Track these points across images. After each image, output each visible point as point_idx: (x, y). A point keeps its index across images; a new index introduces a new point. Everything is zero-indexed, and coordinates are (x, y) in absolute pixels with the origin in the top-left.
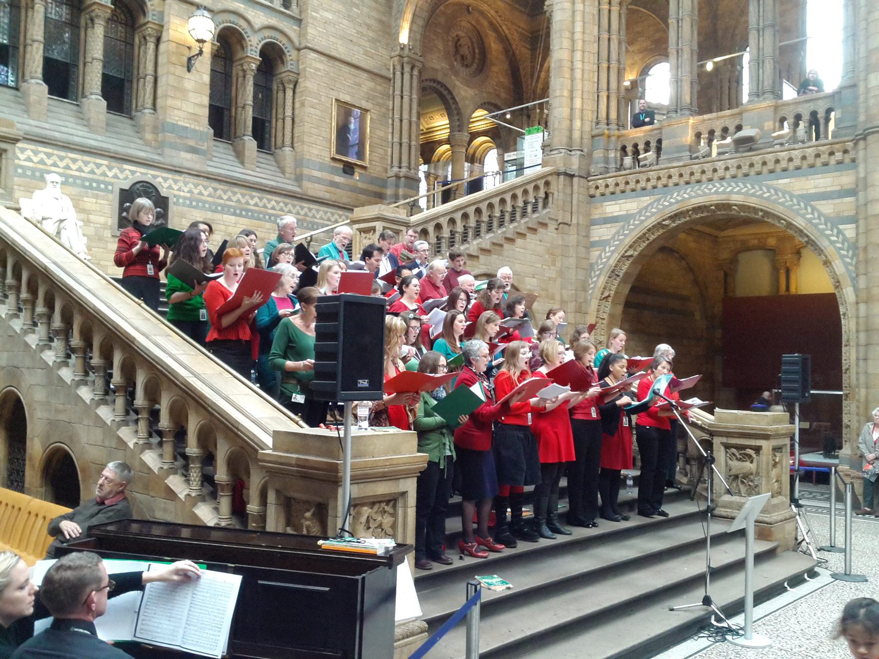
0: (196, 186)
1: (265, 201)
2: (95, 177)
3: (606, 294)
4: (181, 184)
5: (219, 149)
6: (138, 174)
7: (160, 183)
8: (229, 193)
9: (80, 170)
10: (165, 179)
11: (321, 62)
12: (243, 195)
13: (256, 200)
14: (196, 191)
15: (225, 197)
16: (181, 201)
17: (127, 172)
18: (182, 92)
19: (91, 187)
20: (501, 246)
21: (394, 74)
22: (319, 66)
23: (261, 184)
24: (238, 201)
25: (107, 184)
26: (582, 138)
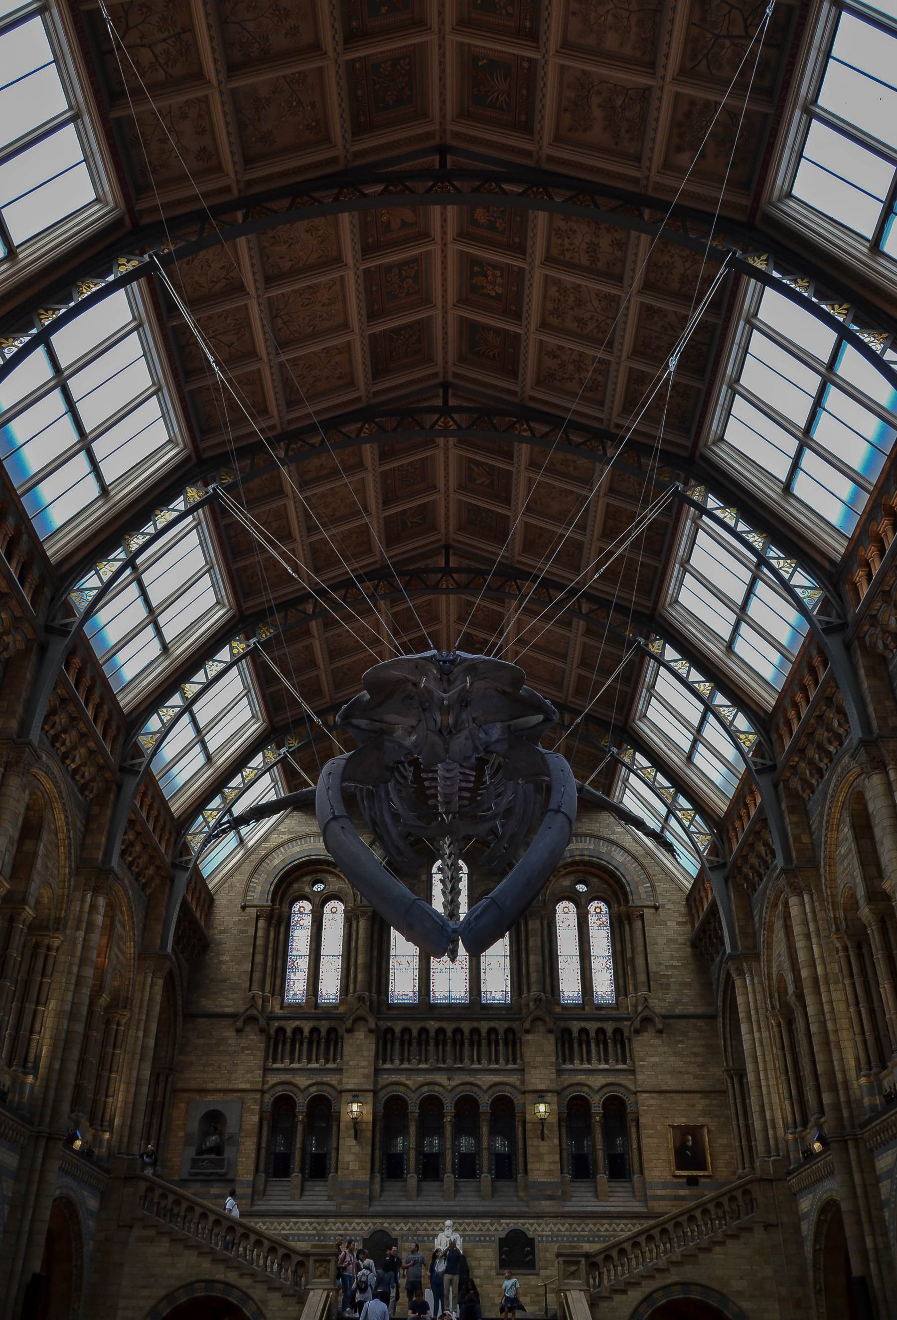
0: (555, 1225)
1: (614, 1225)
4: (543, 1226)
7: (528, 1228)
8: (583, 1225)
10: (532, 1224)
11: (653, 1098)
12: (595, 1225)
13: (606, 1226)
14: (555, 1229)
15: (579, 1229)
16: (544, 1239)
17: (504, 1225)
18: (539, 1157)
19: (480, 1241)
22: (651, 1102)
23: (609, 1212)
24: (591, 1230)
25: (490, 1236)
26: (777, 1144)
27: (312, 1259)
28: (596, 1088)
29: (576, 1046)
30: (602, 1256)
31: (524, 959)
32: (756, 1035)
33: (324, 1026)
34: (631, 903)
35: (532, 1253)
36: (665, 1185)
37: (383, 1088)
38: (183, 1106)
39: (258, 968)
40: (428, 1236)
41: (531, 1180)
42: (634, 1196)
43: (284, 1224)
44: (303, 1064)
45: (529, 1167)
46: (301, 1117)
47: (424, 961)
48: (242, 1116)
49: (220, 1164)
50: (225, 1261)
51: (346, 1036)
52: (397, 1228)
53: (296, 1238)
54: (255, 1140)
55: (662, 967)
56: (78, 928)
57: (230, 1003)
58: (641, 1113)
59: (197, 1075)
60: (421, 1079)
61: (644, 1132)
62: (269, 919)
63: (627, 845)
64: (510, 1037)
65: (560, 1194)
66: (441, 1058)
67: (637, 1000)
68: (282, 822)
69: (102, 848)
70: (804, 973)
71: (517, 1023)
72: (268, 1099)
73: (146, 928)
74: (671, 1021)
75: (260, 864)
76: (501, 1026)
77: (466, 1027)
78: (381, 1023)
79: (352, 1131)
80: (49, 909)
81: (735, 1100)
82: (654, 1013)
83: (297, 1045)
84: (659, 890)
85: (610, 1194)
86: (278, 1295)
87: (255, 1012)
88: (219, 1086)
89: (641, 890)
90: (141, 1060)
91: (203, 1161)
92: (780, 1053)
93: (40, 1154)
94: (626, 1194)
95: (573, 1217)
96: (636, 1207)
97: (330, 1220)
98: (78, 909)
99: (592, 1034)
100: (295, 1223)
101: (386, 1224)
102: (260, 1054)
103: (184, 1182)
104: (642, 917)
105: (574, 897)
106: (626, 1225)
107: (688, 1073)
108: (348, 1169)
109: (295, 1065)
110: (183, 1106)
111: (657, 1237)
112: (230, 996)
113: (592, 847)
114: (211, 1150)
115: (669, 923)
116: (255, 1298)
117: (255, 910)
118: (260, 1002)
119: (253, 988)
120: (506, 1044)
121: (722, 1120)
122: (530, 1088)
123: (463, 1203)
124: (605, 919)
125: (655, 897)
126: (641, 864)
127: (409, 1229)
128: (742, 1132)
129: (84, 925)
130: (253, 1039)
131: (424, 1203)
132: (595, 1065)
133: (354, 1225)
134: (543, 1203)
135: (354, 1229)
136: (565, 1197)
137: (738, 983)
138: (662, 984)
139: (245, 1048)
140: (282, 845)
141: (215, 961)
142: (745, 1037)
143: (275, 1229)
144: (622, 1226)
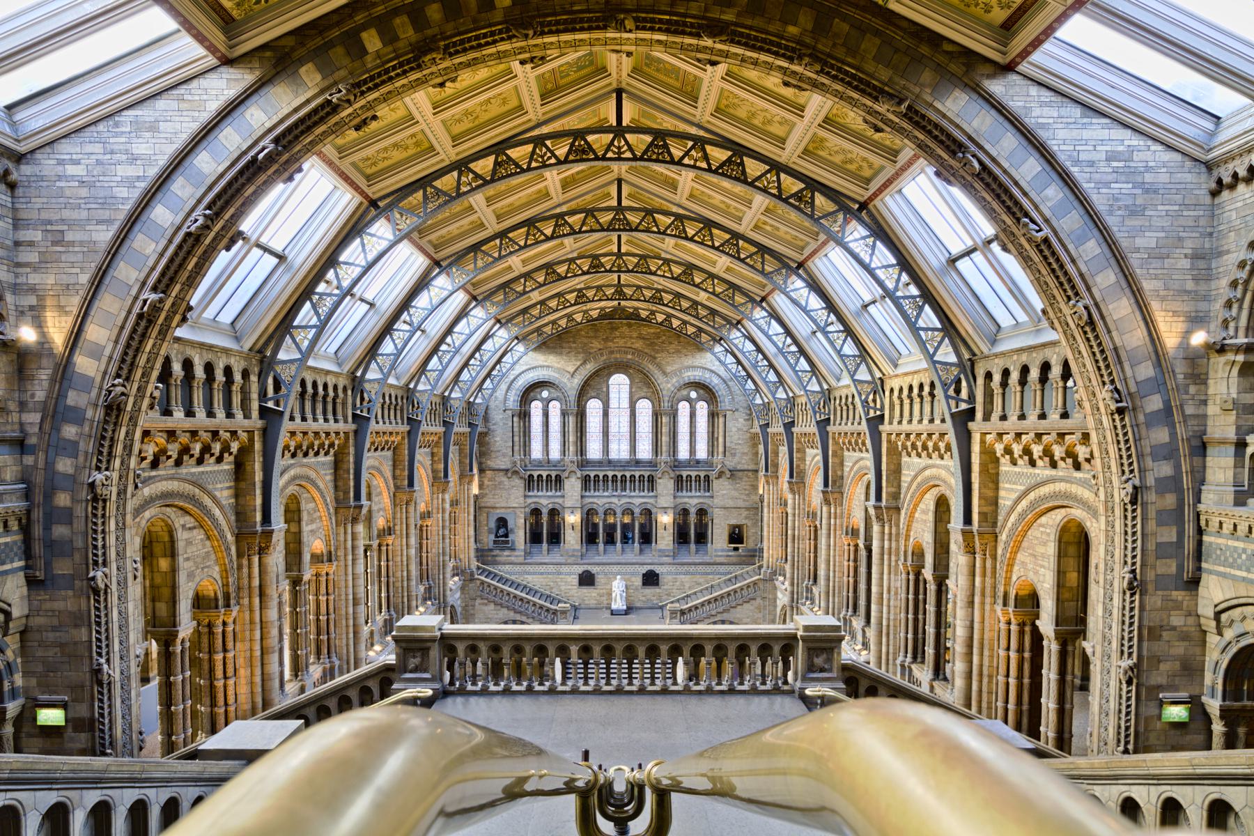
18: (663, 538)
33: (553, 474)
44: (544, 493)
49: (507, 542)
50: (520, 613)
52: (594, 569)
60: (605, 500)
62: (520, 416)
70: (790, 532)
72: (528, 510)
76: (646, 474)
77: (628, 474)
96: (707, 559)
101: (589, 568)
102: (522, 489)
105: (688, 400)
124: (705, 412)
136: (674, 557)
142: (765, 514)
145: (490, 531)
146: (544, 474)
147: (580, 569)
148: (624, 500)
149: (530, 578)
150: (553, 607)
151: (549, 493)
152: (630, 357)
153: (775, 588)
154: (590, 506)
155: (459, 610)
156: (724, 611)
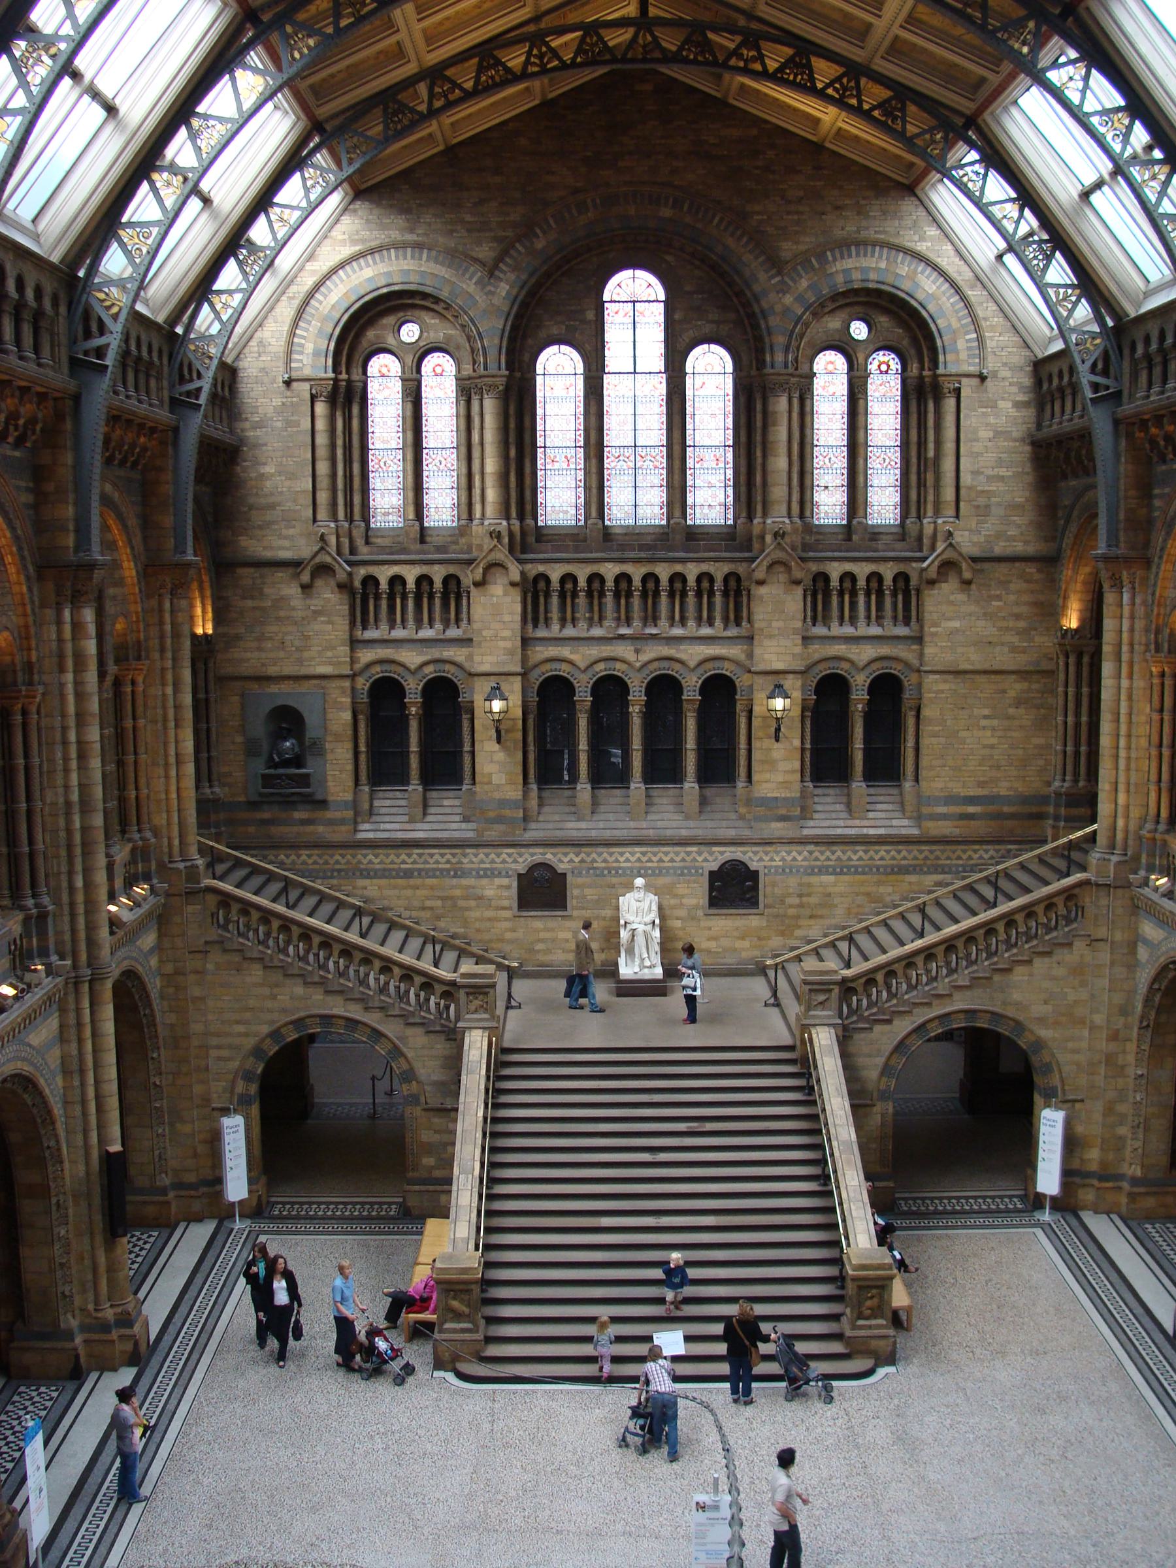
0: (789, 853)
1: (871, 853)
2: (687, 864)
3: (1145, 1024)
5: (829, 799)
6: (727, 854)
9: (672, 861)
11: (945, 681)
12: (844, 852)
13: (861, 853)
14: (789, 858)
18: (771, 763)
19: (682, 874)
20: (986, 978)
21: (1058, 664)
24: (839, 859)
26: (1126, 839)
27: (462, 992)
28: (861, 664)
29: (835, 600)
30: (863, 980)
31: (759, 461)
32: (1125, 683)
33: (438, 574)
34: (941, 370)
35: (755, 888)
36: (951, 800)
37: (536, 666)
38: (236, 698)
39: (323, 482)
40: (609, 869)
41: (757, 795)
42: (903, 811)
43: (403, 857)
45: (755, 777)
46: (413, 710)
47: (594, 461)
48: (325, 713)
49: (305, 780)
51: (473, 591)
52: (563, 861)
53: (423, 873)
54: (349, 745)
55: (982, 478)
56: (62, 669)
57: (286, 543)
58: (925, 701)
59: (249, 655)
60: (594, 652)
61: (925, 729)
62: (332, 400)
63: (943, 262)
64: (732, 583)
65: (798, 812)
66: (623, 616)
67: (935, 529)
68: (337, 221)
69: (71, 527)
71: (745, 565)
72: (363, 684)
73: (147, 523)
74: (986, 566)
75: (306, 302)
76: (719, 571)
77: (664, 572)
78: (529, 566)
79: (493, 733)
80: (12, 654)
81: (1066, 686)
82: (960, 554)
83: (398, 601)
84: (990, 344)
85: (869, 807)
86: (420, 1031)
87: (328, 559)
88: (288, 670)
89: (961, 345)
90: (177, 726)
91: (279, 777)
92: (1156, 717)
93: (86, 1004)
94: (890, 807)
95: (817, 844)
96: (904, 826)
97: (468, 851)
98: (54, 636)
99: (861, 583)
100: (420, 855)
101: (549, 856)
102: (343, 624)
103: (253, 805)
104: (958, 392)
105: (845, 346)
106: (888, 852)
107: (1002, 644)
108: (490, 783)
109: (399, 633)
110: (236, 698)
111: (940, 956)
112: (284, 532)
113: (883, 265)
114: (286, 763)
115: (1001, 404)
116: (390, 1035)
117: (306, 386)
118: (333, 540)
119: (319, 517)
120: (726, 594)
121: (1043, 711)
122: (761, 667)
123: (660, 824)
125: (982, 359)
126: (964, 298)
127: (582, 861)
128: (1070, 732)
129: (70, 663)
130: (328, 596)
131: (601, 825)
132: (863, 630)
133: (504, 856)
134: (774, 825)
135: (504, 862)
137: (1109, 598)
138: (978, 507)
139: (317, 613)
140: (342, 265)
141: (253, 475)
142: (1107, 681)
143: (392, 862)
144: (882, 853)
145: (251, 749)
146: (411, 574)
147: (522, 861)
148: (652, 652)
149: (371, 888)
150: (443, 973)
151: (426, 633)
152: (666, 212)
153: (1138, 908)
154: (549, 670)
155: (154, 985)
156: (975, 982)
